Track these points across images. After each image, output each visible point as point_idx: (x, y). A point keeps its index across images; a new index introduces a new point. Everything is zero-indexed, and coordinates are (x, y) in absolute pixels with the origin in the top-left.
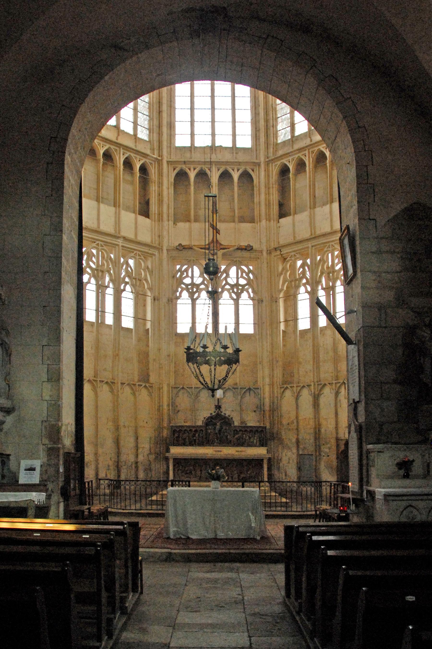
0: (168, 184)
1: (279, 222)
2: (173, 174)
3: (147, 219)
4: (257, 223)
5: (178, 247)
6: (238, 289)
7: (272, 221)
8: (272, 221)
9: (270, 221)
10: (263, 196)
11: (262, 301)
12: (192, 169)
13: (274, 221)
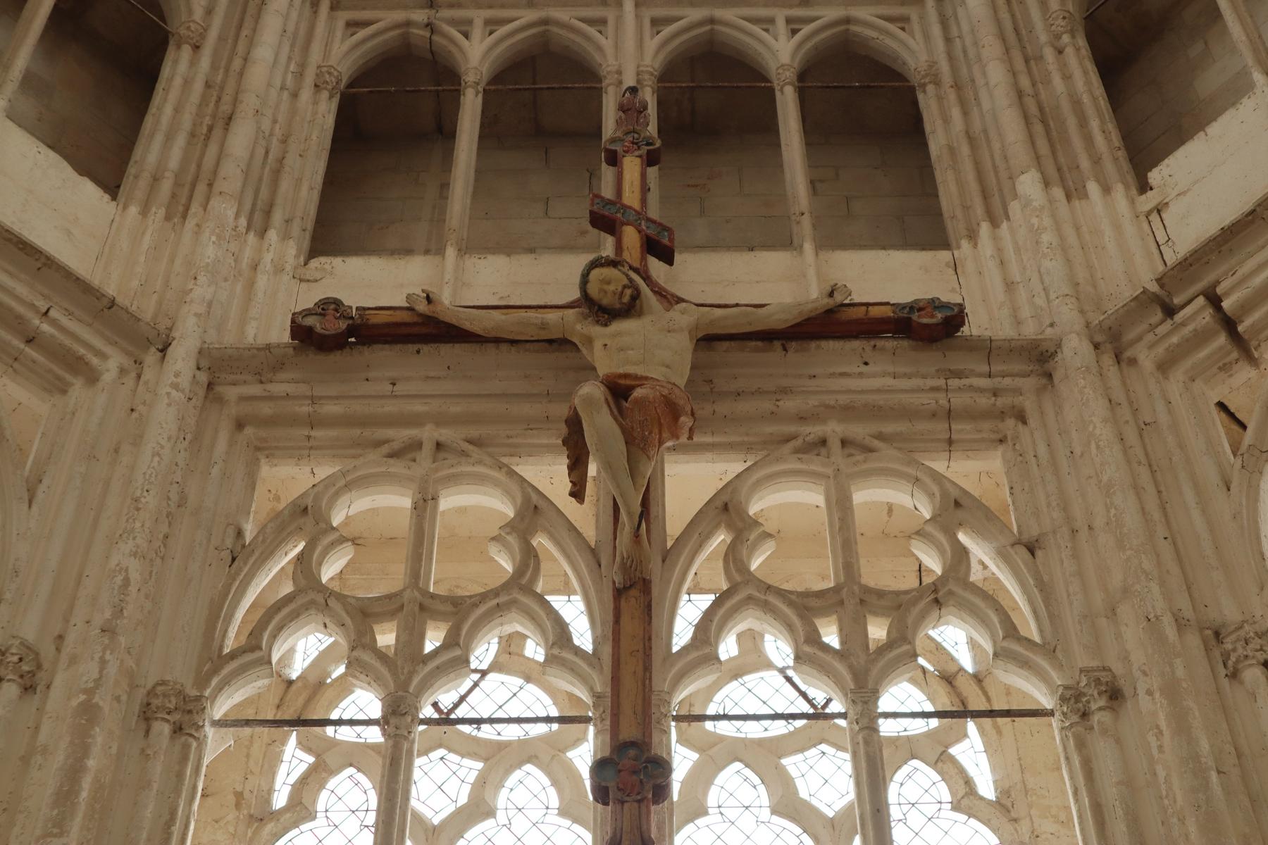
0: (300, 75)
1: (1144, 187)
2: (340, 51)
3: (89, 190)
4: (972, 236)
5: (310, 321)
6: (854, 633)
7: (1093, 188)
8: (1093, 188)
9: (1074, 193)
10: (995, 78)
11: (1115, 695)
12: (477, 32)
13: (1107, 190)
